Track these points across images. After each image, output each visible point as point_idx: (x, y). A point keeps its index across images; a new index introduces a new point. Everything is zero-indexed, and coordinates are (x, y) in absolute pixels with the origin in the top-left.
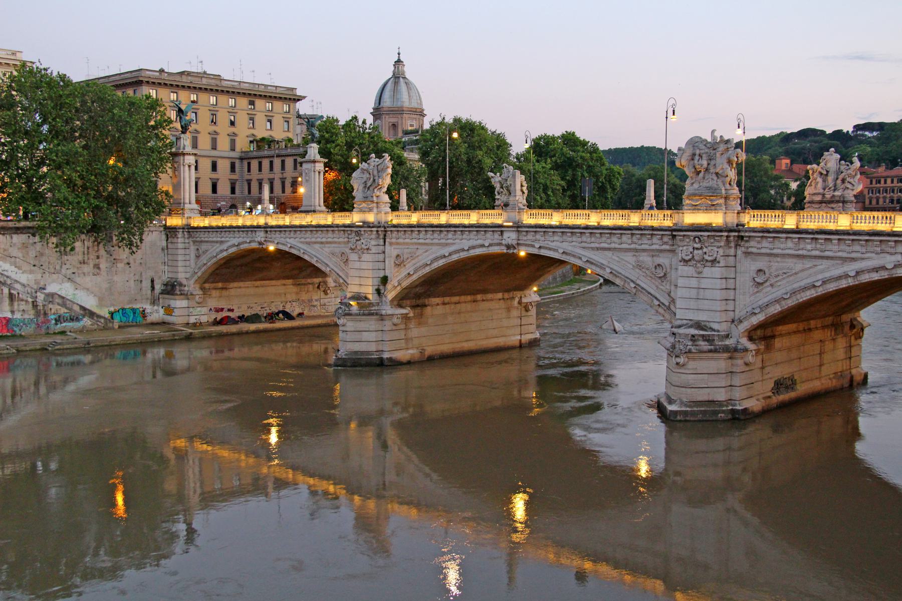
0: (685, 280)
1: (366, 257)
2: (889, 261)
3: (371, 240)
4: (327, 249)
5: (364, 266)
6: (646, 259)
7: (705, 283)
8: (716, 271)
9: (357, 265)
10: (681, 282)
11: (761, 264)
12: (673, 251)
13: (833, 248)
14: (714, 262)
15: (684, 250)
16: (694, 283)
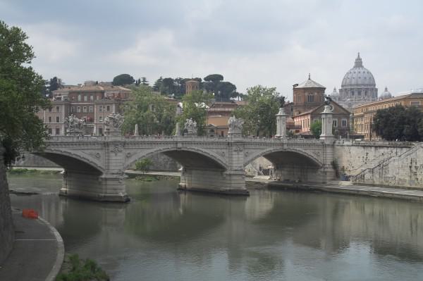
0: (235, 156)
1: (119, 154)
2: (272, 149)
3: (120, 148)
4: (86, 151)
5: (118, 158)
6: (219, 151)
7: (240, 156)
8: (242, 153)
9: (114, 158)
10: (234, 156)
11: (246, 151)
12: (226, 149)
13: (262, 147)
14: (241, 151)
15: (234, 148)
16: (237, 156)
